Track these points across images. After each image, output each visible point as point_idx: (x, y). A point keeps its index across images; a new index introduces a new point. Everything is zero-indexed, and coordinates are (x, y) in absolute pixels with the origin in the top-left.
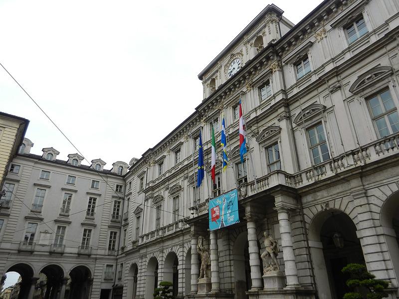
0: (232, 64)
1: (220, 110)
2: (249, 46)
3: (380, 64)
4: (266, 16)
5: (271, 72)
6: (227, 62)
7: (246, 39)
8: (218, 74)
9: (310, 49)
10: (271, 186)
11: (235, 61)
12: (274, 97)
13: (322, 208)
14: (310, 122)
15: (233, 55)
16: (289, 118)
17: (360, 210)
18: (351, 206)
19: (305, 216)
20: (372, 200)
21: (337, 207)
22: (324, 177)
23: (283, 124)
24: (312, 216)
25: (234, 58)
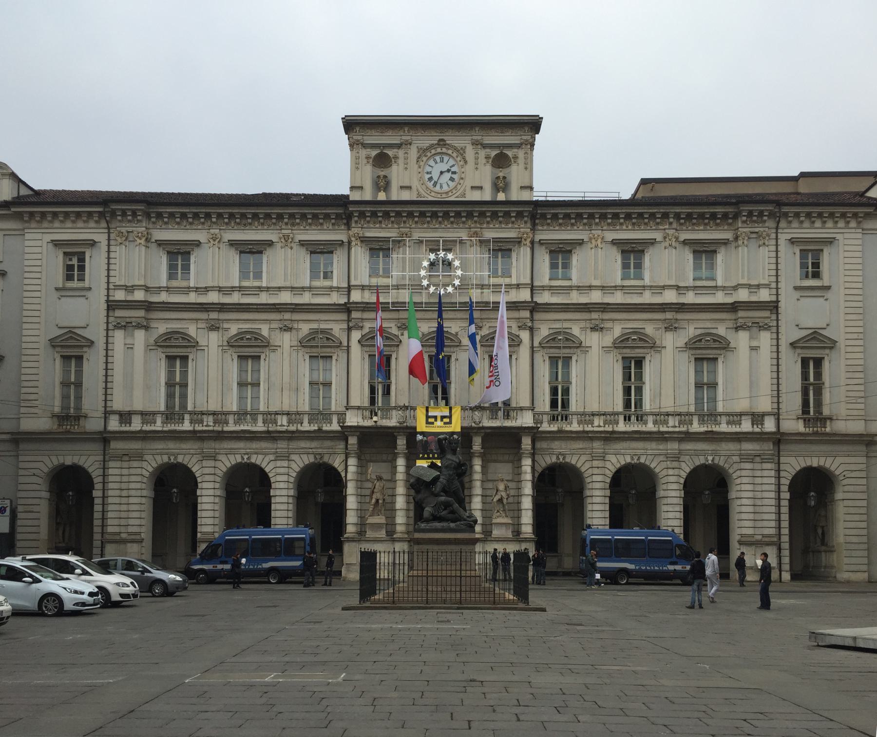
0: (438, 158)
2: (483, 153)
7: (477, 135)
8: (401, 153)
11: (446, 158)
12: (518, 286)
15: (442, 143)
16: (531, 329)
17: (596, 471)
18: (587, 465)
20: (608, 465)
21: (573, 462)
22: (568, 428)
23: (525, 335)
24: (544, 465)
25: (444, 150)
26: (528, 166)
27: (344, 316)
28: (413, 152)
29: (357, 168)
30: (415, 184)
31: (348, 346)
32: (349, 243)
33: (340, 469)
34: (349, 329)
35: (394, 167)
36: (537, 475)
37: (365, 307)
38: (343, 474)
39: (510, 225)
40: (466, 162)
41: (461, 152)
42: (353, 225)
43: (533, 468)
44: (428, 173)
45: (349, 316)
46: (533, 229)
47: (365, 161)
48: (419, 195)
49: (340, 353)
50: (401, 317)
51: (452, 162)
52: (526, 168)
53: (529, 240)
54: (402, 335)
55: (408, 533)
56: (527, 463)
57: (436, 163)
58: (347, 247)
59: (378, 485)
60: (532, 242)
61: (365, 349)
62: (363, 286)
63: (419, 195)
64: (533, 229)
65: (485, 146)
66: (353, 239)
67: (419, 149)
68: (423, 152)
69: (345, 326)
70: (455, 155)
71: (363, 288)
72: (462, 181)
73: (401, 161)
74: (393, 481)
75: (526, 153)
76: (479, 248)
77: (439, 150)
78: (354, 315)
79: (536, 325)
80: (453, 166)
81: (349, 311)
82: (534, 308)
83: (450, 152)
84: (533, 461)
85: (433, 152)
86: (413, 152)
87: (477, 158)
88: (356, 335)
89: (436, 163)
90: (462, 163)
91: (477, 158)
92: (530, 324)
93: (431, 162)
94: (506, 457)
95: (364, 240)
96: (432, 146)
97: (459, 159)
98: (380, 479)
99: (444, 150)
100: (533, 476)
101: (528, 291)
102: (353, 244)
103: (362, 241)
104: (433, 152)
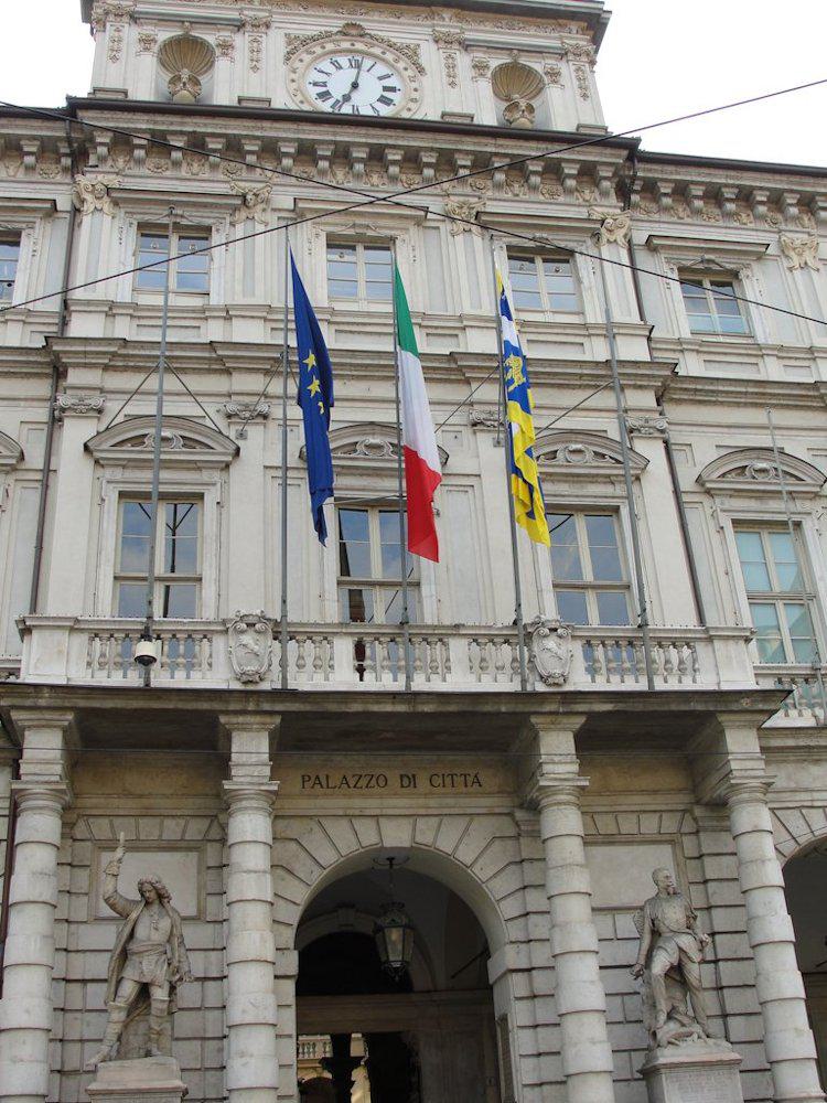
0: (343, 60)
2: (464, 61)
3: (606, 431)
4: (574, 26)
6: (313, 31)
8: (241, 41)
9: (755, 266)
10: (705, 682)
11: (367, 63)
14: (753, 504)
15: (350, 30)
25: (359, 46)
26: (586, 92)
27: (42, 388)
28: (274, 43)
31: (48, 471)
32: (76, 211)
34: (55, 421)
35: (222, 65)
37: (119, 356)
40: (421, 70)
41: (410, 54)
44: (315, 84)
45: (56, 389)
49: (17, 492)
50: (237, 387)
51: (381, 69)
52: (585, 96)
54: (242, 435)
61: (108, 473)
62: (112, 305)
65: (466, 46)
66: (88, 197)
67: (290, 39)
68: (296, 46)
69: (42, 413)
70: (389, 57)
71: (111, 309)
74: (214, 912)
75: (577, 70)
77: (346, 45)
78: (74, 377)
81: (58, 372)
82: (669, 387)
83: (377, 51)
85: (330, 46)
86: (274, 43)
88: (76, 432)
93: (326, 65)
94: (650, 825)
95: (118, 198)
96: (328, 35)
97: (401, 65)
99: (359, 46)
102: (88, 207)
103: (116, 203)
104: (330, 46)
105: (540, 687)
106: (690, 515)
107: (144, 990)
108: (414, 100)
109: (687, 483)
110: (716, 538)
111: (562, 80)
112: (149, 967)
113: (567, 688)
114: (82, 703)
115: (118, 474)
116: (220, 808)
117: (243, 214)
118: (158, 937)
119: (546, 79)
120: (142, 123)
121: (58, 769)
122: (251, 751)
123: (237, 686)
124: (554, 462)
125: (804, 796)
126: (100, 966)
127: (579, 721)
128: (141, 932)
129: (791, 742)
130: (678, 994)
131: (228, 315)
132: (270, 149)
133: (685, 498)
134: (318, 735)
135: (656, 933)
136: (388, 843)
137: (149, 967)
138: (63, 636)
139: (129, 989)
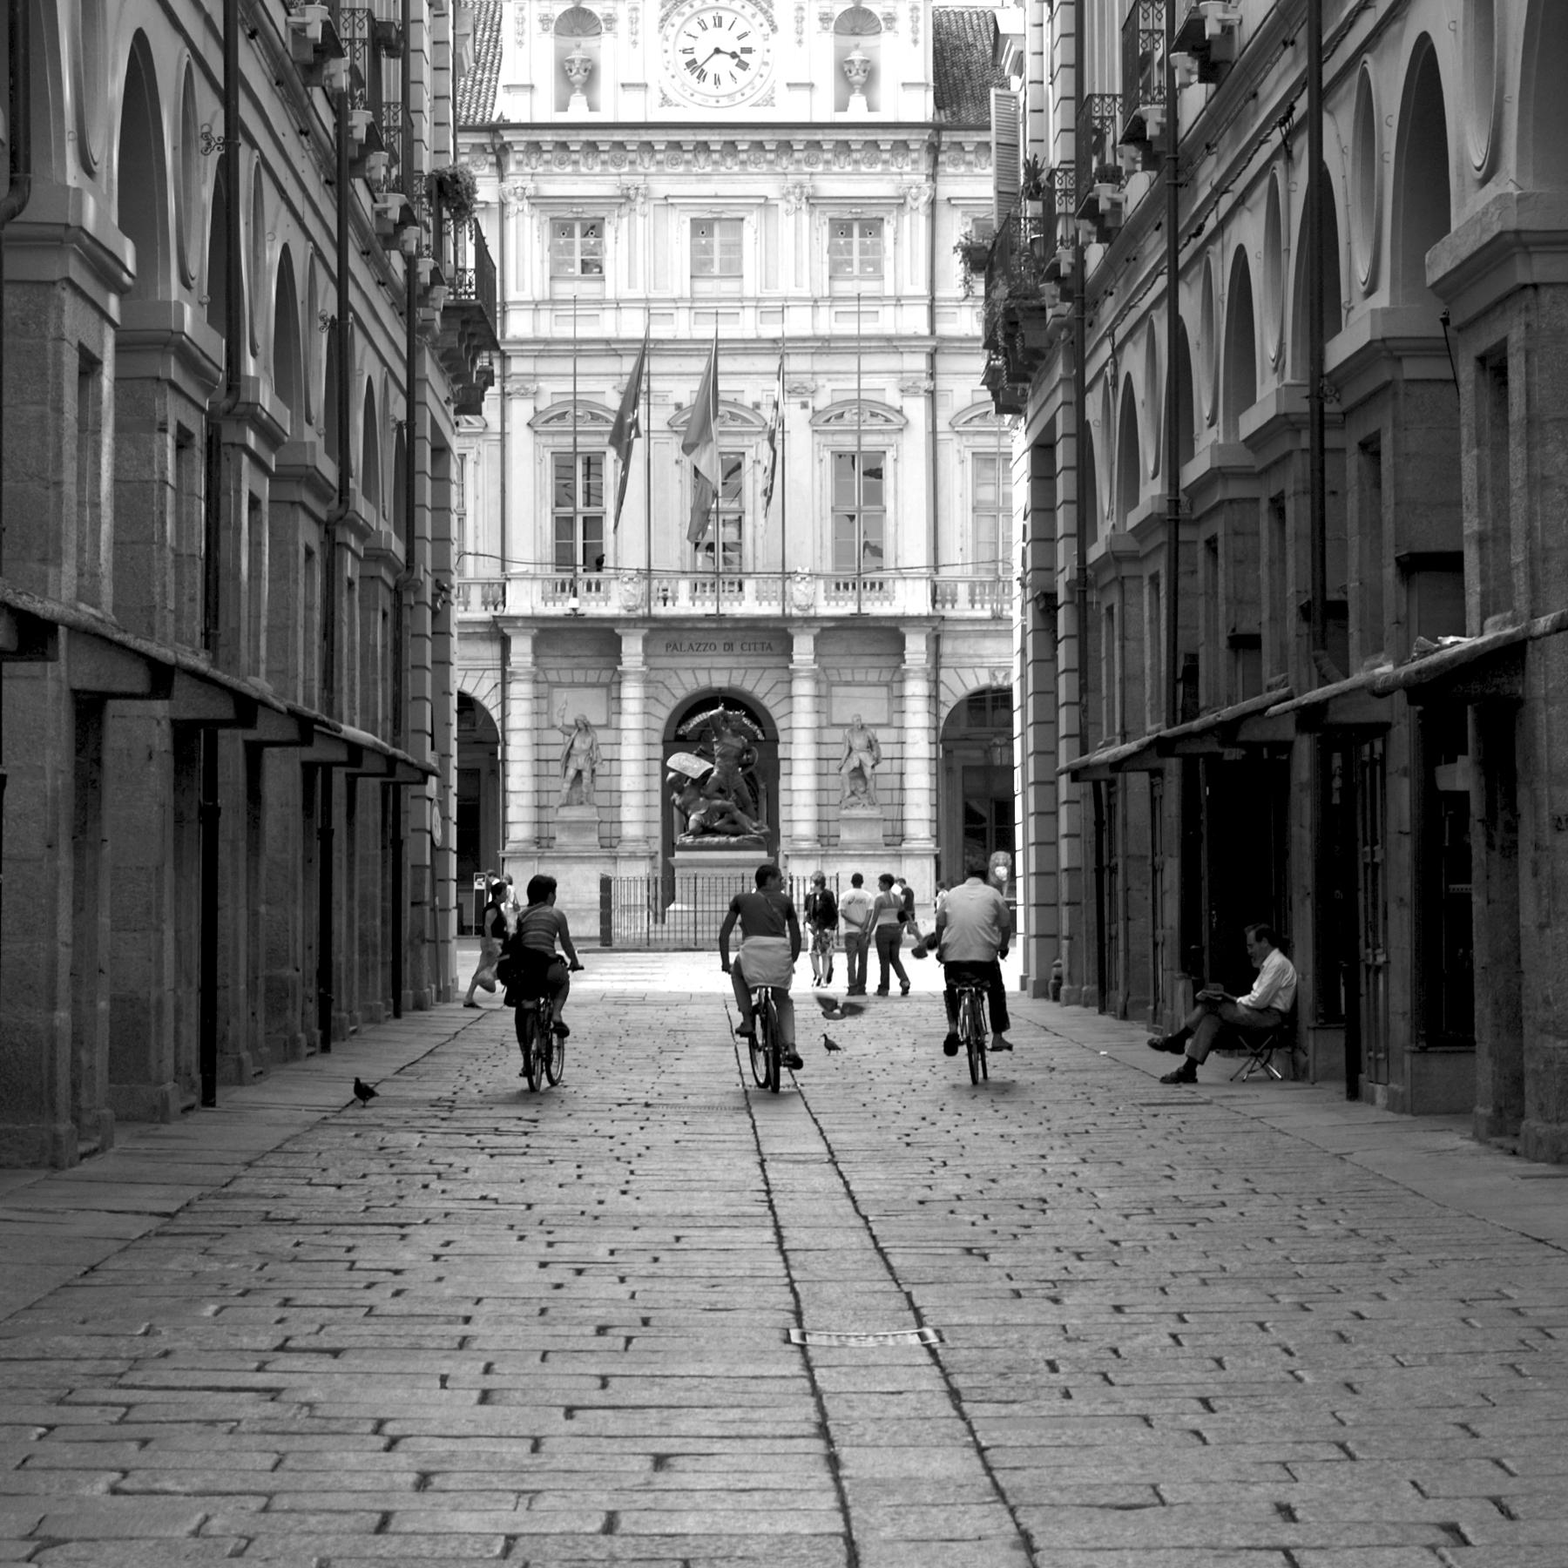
1: (628, 197)
5: (900, 203)
12: (898, 301)
13: (993, 676)
16: (932, 394)
19: (942, 687)
23: (916, 409)
29: (521, 43)
30: (656, 77)
31: (503, 434)
32: (503, 205)
33: (491, 703)
35: (606, 38)
36: (945, 712)
38: (496, 714)
39: (879, 168)
40: (774, 29)
42: (512, 168)
43: (934, 698)
46: (933, 177)
47: (538, 27)
48: (665, 101)
53: (924, 199)
55: (648, 839)
56: (916, 688)
57: (705, 28)
58: (497, 216)
59: (581, 744)
60: (933, 203)
62: (537, 303)
63: (665, 101)
64: (933, 177)
66: (512, 199)
72: (765, 70)
73: (622, 26)
76: (805, 218)
79: (943, 383)
80: (745, 35)
84: (936, 682)
87: (800, 20)
89: (705, 28)
90: (767, 28)
91: (800, 20)
92: (927, 384)
94: (873, 676)
95: (538, 201)
98: (584, 727)
100: (937, 716)
101: (923, 311)
102: (511, 209)
105: (795, 612)
106: (941, 448)
107: (579, 773)
108: (766, 64)
109: (942, 425)
110: (959, 467)
111: (898, 25)
112: (579, 762)
113: (812, 612)
114: (541, 625)
115: (549, 440)
116: (617, 681)
117: (625, 210)
118: (585, 747)
119: (883, 24)
120: (548, 136)
121: (530, 659)
122: (632, 648)
123: (623, 613)
124: (840, 421)
125: (977, 660)
126: (558, 752)
127: (817, 631)
128: (576, 744)
129: (969, 628)
130: (860, 782)
131: (618, 305)
132: (648, 146)
133: (940, 436)
134: (669, 635)
135: (851, 750)
136: (715, 685)
137: (579, 762)
138: (526, 584)
139: (571, 772)
